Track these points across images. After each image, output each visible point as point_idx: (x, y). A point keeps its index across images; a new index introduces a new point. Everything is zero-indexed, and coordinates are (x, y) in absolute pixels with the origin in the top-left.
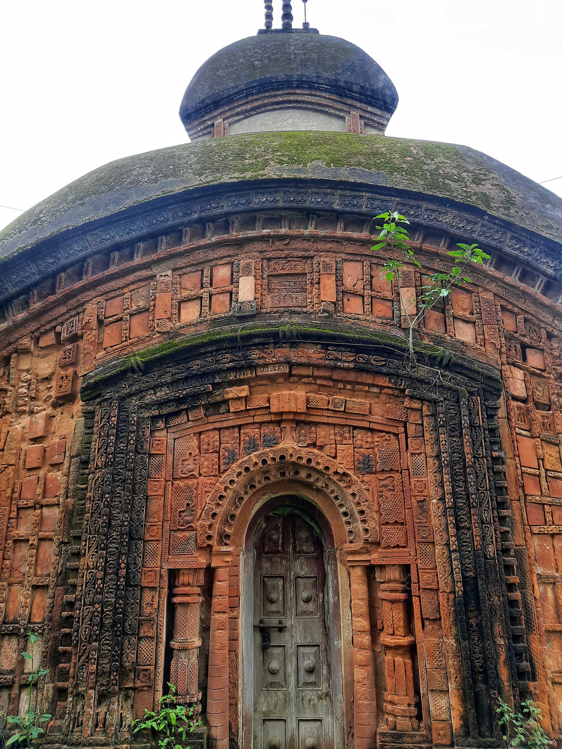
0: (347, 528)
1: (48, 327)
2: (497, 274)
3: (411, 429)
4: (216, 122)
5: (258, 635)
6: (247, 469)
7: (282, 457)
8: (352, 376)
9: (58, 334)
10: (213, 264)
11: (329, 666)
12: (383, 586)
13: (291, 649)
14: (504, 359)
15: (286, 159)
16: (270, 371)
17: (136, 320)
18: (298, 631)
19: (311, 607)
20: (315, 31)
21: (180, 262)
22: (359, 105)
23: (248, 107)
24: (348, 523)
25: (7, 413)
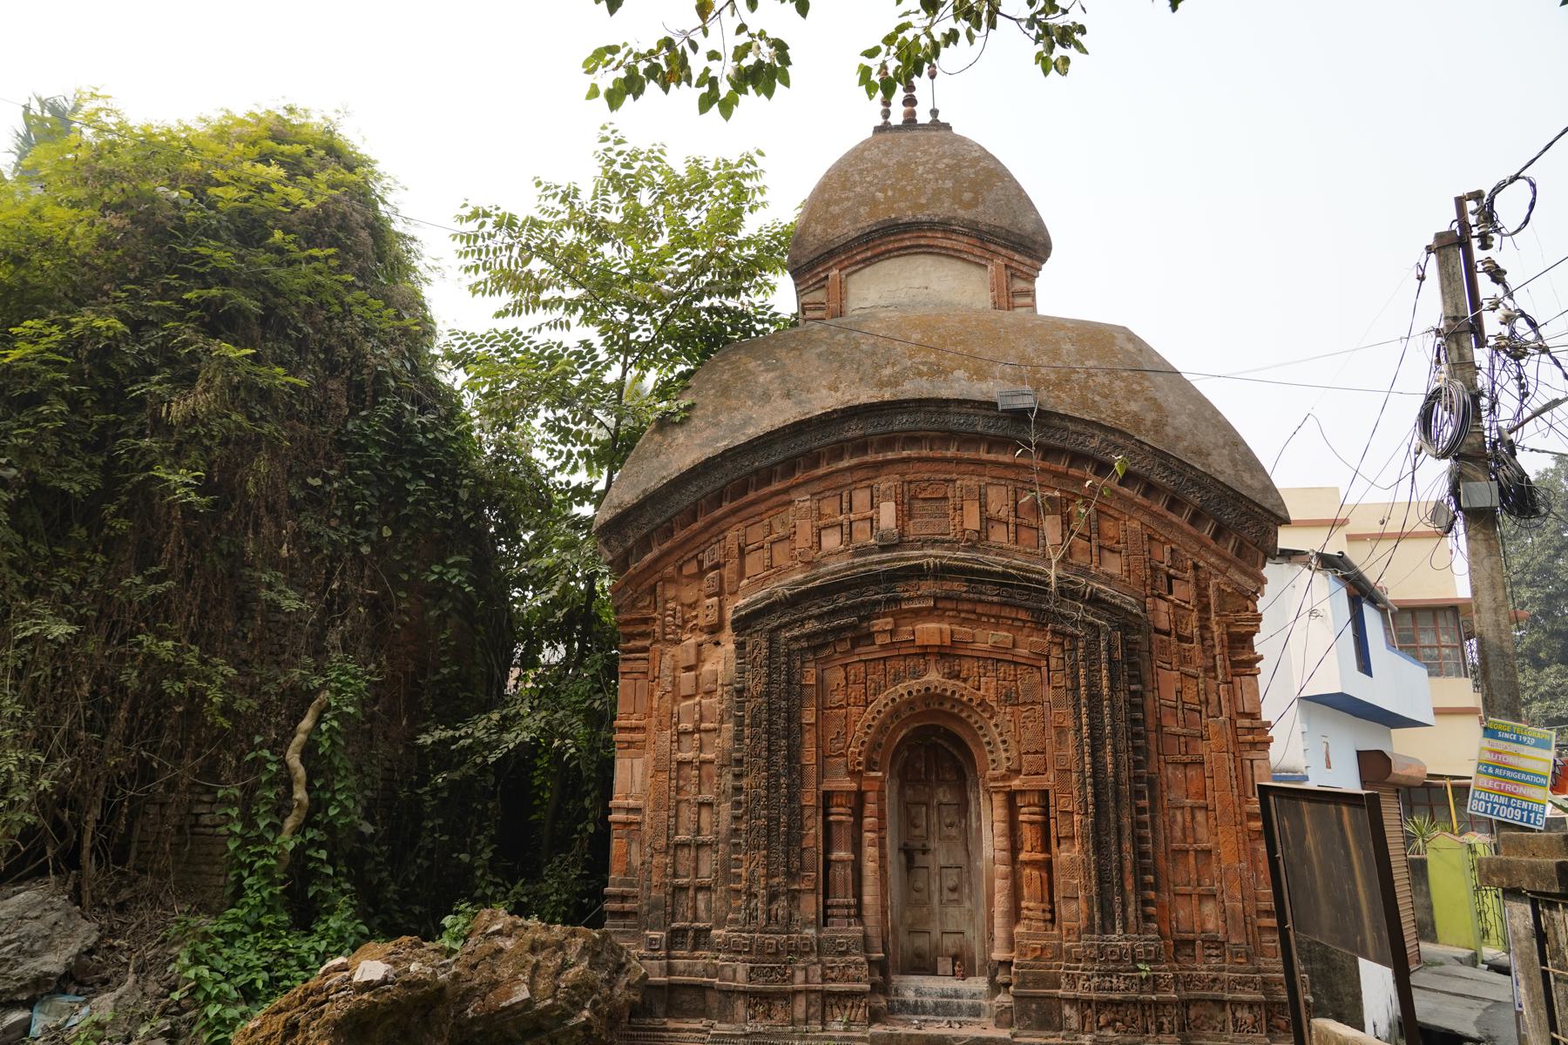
0: (990, 757)
2: (1146, 502)
3: (1053, 662)
6: (893, 700)
7: (928, 689)
9: (701, 563)
12: (1024, 810)
13: (934, 869)
15: (925, 369)
16: (916, 605)
17: (777, 547)
18: (940, 855)
19: (953, 832)
20: (947, 127)
21: (817, 487)
22: (1004, 251)
23: (869, 254)
25: (656, 641)
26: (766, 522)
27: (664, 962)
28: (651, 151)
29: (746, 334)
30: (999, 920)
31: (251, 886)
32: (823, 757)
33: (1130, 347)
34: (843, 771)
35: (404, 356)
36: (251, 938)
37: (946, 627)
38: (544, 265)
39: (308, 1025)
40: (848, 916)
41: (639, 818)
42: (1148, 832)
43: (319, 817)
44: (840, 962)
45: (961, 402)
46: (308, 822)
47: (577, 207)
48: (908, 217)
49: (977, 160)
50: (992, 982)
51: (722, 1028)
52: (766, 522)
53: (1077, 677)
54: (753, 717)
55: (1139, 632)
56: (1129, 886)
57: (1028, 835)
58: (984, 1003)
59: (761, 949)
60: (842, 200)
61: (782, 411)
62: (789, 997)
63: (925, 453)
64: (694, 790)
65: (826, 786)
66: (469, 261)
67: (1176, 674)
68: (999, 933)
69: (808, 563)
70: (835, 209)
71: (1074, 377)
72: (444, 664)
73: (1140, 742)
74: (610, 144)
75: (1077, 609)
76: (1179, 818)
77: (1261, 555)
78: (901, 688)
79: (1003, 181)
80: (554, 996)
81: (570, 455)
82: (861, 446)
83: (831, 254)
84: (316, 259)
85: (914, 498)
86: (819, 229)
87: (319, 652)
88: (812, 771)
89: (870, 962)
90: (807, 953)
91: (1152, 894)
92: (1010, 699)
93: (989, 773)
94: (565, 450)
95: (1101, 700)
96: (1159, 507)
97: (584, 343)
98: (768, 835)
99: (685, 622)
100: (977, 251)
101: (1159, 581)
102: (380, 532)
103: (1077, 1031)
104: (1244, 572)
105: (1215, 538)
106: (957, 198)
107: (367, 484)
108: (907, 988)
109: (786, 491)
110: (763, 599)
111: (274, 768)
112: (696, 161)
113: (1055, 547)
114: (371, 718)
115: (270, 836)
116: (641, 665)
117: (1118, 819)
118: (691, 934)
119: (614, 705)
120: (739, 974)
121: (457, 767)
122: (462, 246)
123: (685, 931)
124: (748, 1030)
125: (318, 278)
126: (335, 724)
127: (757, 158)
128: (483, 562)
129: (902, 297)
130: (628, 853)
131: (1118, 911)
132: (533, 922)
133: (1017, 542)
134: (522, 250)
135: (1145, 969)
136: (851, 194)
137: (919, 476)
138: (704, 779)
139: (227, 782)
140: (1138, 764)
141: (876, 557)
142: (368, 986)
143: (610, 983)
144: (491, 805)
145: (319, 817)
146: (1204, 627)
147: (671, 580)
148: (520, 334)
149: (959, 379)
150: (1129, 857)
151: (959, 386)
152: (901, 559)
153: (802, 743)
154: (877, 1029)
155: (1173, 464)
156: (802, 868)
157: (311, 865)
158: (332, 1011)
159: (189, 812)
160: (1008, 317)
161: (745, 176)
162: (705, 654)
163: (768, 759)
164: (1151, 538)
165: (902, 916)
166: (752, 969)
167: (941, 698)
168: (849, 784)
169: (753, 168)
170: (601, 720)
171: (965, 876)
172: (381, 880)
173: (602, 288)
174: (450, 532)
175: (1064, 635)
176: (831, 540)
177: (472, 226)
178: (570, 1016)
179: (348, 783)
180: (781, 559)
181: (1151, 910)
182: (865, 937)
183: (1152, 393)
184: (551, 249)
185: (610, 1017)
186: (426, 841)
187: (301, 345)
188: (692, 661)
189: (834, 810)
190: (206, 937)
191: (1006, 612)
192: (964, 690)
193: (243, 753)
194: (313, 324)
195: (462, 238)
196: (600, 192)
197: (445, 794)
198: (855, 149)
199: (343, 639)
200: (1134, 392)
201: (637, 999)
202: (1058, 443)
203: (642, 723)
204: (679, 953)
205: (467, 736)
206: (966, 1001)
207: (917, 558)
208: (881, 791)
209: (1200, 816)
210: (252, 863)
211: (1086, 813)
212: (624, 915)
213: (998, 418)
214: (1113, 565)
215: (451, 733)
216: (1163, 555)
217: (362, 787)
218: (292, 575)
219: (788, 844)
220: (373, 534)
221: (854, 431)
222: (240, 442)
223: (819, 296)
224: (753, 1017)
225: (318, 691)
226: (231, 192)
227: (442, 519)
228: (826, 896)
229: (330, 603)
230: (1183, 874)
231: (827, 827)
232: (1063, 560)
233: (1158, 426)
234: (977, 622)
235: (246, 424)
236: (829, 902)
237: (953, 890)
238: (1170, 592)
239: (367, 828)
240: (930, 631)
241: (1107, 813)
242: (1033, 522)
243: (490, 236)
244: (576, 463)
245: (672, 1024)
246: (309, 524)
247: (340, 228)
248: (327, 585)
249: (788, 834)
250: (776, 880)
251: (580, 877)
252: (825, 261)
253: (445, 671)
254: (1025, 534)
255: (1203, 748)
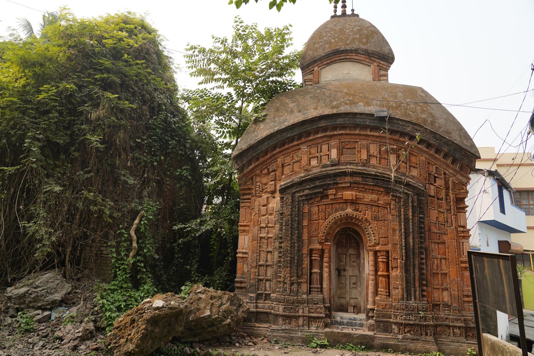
0: (368, 239)
1: (265, 167)
2: (427, 150)
3: (392, 206)
4: (315, 69)
5: (337, 272)
7: (347, 215)
8: (372, 188)
9: (268, 169)
10: (322, 144)
11: (360, 282)
13: (348, 277)
14: (427, 182)
15: (348, 102)
16: (343, 185)
17: (295, 165)
18: (350, 272)
19: (355, 264)
20: (357, 15)
21: (309, 144)
23: (329, 61)
24: (369, 237)
25: (253, 196)
26: (291, 155)
27: (255, 304)
28: (252, 26)
29: (285, 90)
30: (370, 295)
31: (119, 274)
32: (310, 237)
33: (423, 94)
34: (317, 242)
35: (168, 98)
36: (119, 291)
37: (354, 193)
38: (215, 66)
39: (138, 320)
40: (318, 291)
41: (247, 256)
42: (424, 267)
43: (141, 252)
44: (315, 306)
45: (361, 114)
46: (137, 254)
47: (226, 46)
48: (343, 48)
49: (368, 27)
50: (367, 315)
51: (274, 327)
52: (291, 155)
53: (400, 211)
54: (286, 223)
55: (423, 196)
56: (417, 284)
57: (381, 266)
58: (364, 322)
59: (288, 301)
60: (319, 42)
61: (298, 117)
62: (297, 318)
63: (348, 132)
64: (265, 247)
65: (311, 247)
66: (190, 65)
67: (436, 211)
68: (370, 299)
69: (306, 170)
70: (317, 46)
71: (402, 105)
72: (182, 203)
73: (423, 235)
74: (238, 23)
75: (401, 188)
76: (436, 262)
77: (469, 170)
78: (338, 214)
79: (377, 35)
80: (218, 314)
81: (224, 132)
82: (325, 129)
83: (315, 61)
84: (138, 64)
85: (343, 148)
86: (311, 53)
87: (140, 198)
88: (306, 242)
89: (325, 307)
90: (304, 303)
91: (425, 288)
92: (376, 219)
93: (368, 244)
94: (222, 130)
95: (409, 220)
96: (432, 152)
97: (229, 93)
98: (291, 263)
99: (263, 190)
100: (367, 60)
101: (431, 179)
102: (160, 158)
103: (397, 334)
104: (462, 176)
105: (452, 163)
106: (360, 41)
107: (156, 141)
108: (338, 316)
109: (298, 145)
110: (290, 182)
111: (126, 236)
112: (268, 29)
113: (394, 166)
114: (158, 220)
115: (125, 258)
116: (248, 204)
117: (414, 261)
118: (264, 295)
119: (238, 218)
120: (280, 309)
121: (186, 237)
122: (187, 59)
123: (262, 294)
124: (283, 328)
125: (139, 70)
126: (146, 222)
127: (289, 27)
128: (194, 169)
129: (340, 77)
130: (243, 267)
131: (413, 293)
132: (211, 289)
133: (380, 164)
134: (207, 61)
135: (422, 314)
136: (323, 40)
137: (345, 140)
138: (269, 243)
139: (111, 240)
140: (421, 243)
141: (330, 168)
142: (157, 308)
143: (237, 310)
144: (197, 250)
145: (141, 252)
146: (447, 195)
147: (258, 175)
148: (207, 90)
149: (360, 106)
150: (417, 275)
151: (360, 108)
152: (338, 169)
153: (303, 232)
154: (327, 330)
155: (438, 137)
156: (302, 274)
157: (139, 268)
158: (146, 316)
159: (99, 249)
160: (378, 84)
161: (286, 34)
162: (270, 201)
163: (291, 237)
164: (428, 163)
165: (336, 292)
166: (285, 308)
167: (352, 218)
168: (319, 247)
169: (288, 31)
170: (234, 223)
171: (358, 279)
172: (161, 274)
173: (235, 75)
174: (183, 158)
175: (396, 197)
176: (314, 162)
177: (191, 52)
178: (224, 321)
179: (150, 241)
180: (296, 168)
181: (425, 293)
182: (324, 298)
183: (431, 111)
184: (218, 60)
185: (237, 322)
186: (176, 262)
187: (134, 94)
188: (265, 203)
189: (313, 255)
190: (105, 290)
191: (376, 188)
192: (360, 215)
193: (116, 231)
194: (137, 87)
195: (187, 57)
196: (235, 40)
197: (182, 246)
198: (324, 24)
199: (148, 193)
200: (424, 111)
201: (246, 316)
202: (396, 129)
203: (248, 224)
204: (260, 301)
205: (189, 227)
206: (358, 322)
207: (344, 169)
208: (330, 249)
209: (443, 261)
210: (120, 267)
211: (402, 259)
212: (241, 288)
213: (374, 120)
214: (415, 172)
215: (184, 226)
216: (433, 169)
217: (155, 243)
218: (131, 172)
219: (298, 266)
220: (158, 159)
221: (323, 124)
222: (114, 127)
223: (311, 77)
224: (285, 324)
225: (140, 211)
226: (110, 41)
227: (181, 154)
228: (310, 284)
229: (144, 182)
230: (437, 281)
231: (311, 261)
232: (396, 170)
233: (432, 123)
234: (365, 191)
235: (116, 121)
236: (311, 286)
237: (354, 284)
238: (435, 182)
239: (157, 257)
240: (348, 194)
241: (410, 259)
242: (386, 157)
243: (197, 56)
244: (226, 135)
245: (257, 325)
246: (137, 155)
247: (146, 54)
248: (143, 175)
249: (297, 263)
250: (293, 278)
251: (227, 275)
252: (313, 64)
253: (182, 205)
254: (383, 161)
255: (445, 238)
